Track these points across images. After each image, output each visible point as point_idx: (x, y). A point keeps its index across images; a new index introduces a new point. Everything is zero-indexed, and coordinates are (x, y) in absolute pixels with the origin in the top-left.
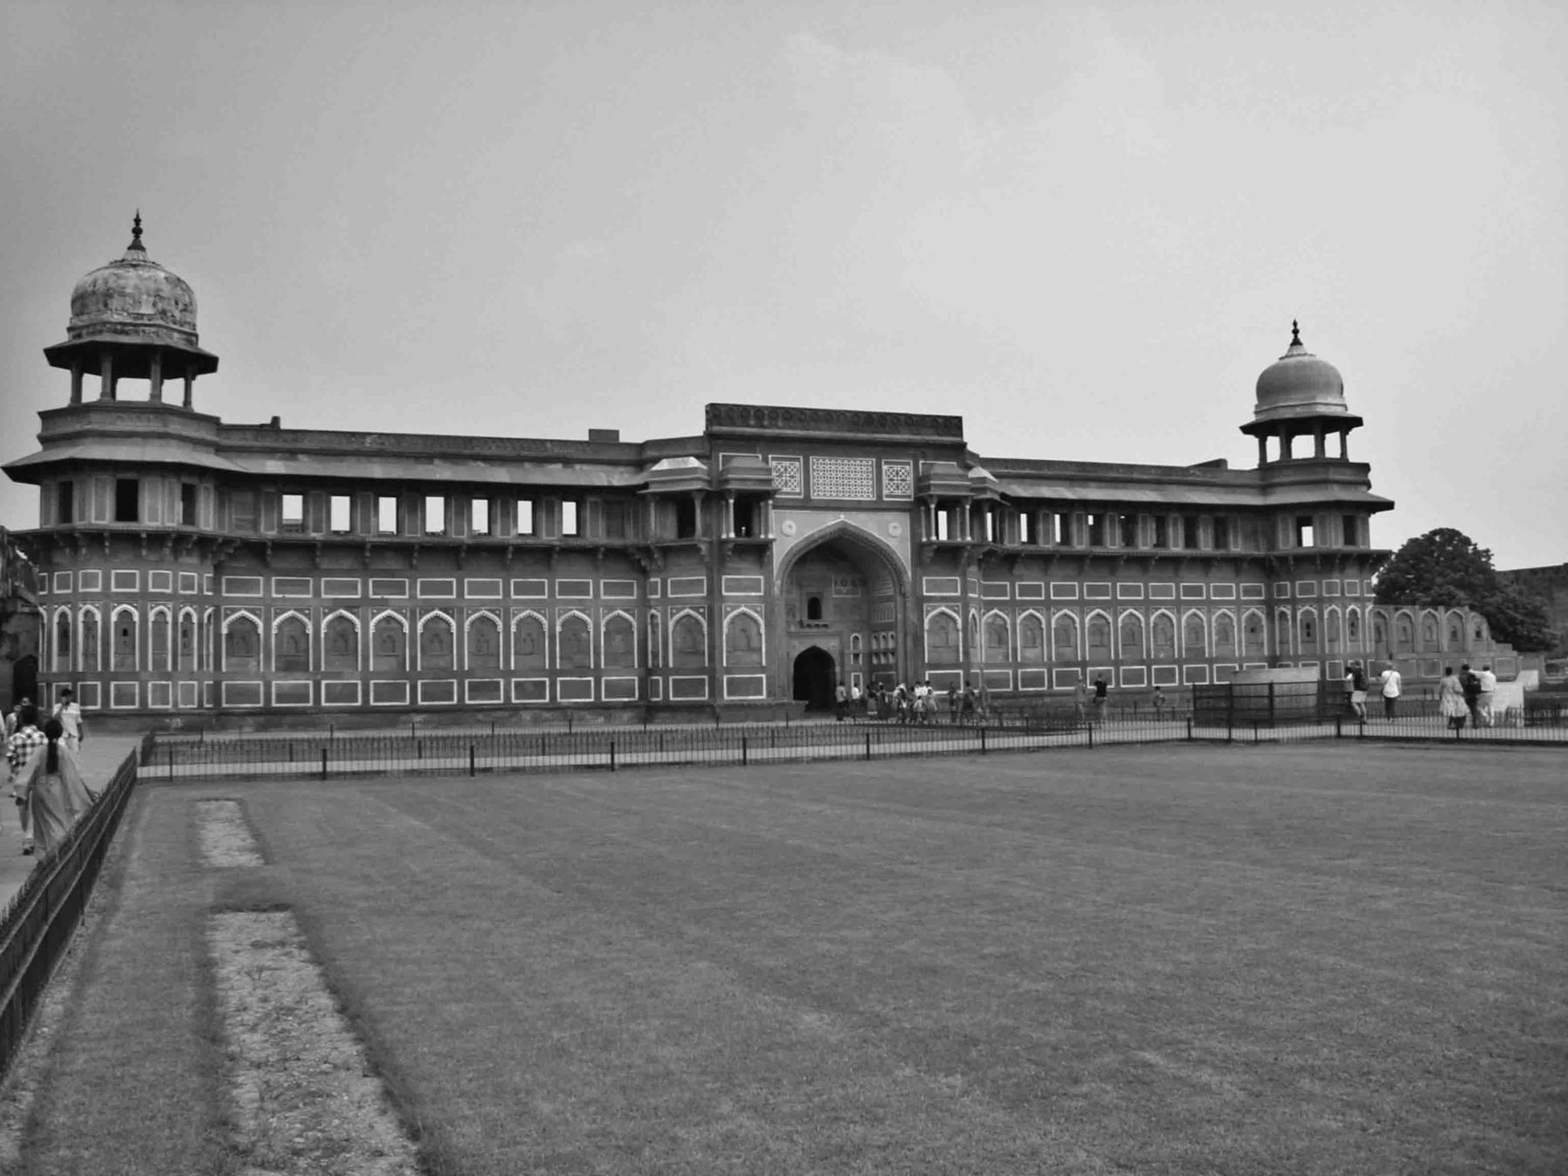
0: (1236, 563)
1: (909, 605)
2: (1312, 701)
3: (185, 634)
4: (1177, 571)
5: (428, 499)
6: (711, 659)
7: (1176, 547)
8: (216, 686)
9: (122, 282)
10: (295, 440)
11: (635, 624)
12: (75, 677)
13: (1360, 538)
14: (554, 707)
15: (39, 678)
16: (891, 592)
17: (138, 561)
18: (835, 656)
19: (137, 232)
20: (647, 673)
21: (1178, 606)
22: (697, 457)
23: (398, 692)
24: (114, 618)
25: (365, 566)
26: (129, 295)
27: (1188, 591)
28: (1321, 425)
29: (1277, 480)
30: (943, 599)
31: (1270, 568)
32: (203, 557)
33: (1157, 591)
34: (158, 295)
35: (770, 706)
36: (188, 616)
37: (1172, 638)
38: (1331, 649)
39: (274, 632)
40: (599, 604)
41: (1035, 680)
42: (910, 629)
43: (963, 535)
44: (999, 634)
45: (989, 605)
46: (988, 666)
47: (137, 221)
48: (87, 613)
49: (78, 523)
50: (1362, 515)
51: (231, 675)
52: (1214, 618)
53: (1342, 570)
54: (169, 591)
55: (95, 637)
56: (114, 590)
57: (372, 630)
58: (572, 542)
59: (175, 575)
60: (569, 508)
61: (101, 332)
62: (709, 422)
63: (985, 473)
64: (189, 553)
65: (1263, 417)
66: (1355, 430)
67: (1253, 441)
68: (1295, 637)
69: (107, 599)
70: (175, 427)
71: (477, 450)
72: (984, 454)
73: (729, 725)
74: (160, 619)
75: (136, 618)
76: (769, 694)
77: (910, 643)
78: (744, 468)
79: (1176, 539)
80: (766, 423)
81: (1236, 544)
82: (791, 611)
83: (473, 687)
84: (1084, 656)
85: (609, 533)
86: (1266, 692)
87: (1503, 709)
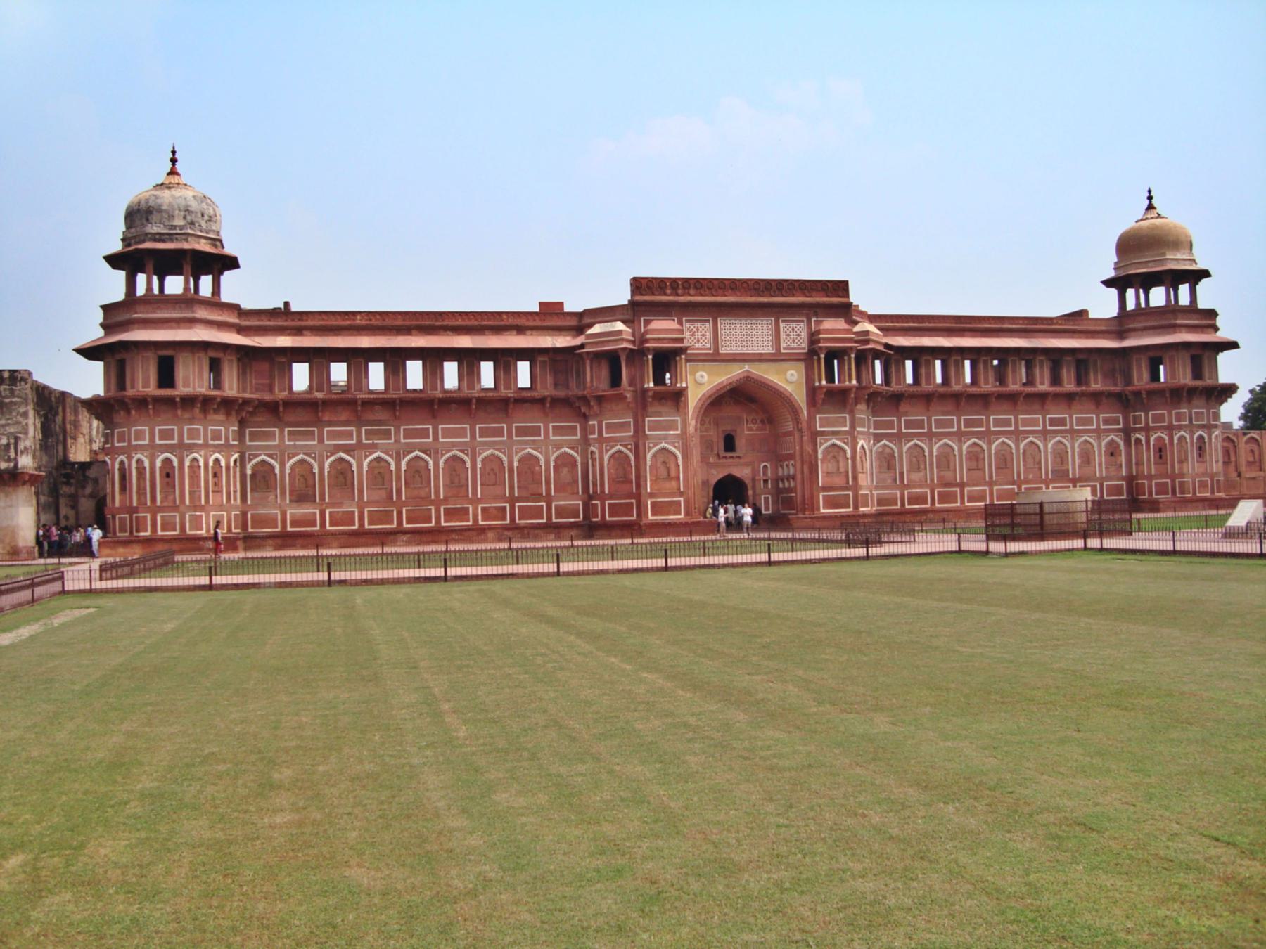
0: (1096, 397)
1: (805, 438)
2: (1082, 518)
3: (215, 475)
4: (1043, 404)
5: (409, 363)
6: (638, 486)
7: (1043, 387)
8: (244, 514)
9: (159, 201)
10: (300, 320)
11: (579, 459)
12: (132, 510)
13: (1206, 374)
14: (513, 527)
15: (107, 511)
16: (790, 428)
17: (176, 420)
18: (747, 482)
19: (174, 161)
20: (588, 498)
21: (1045, 434)
22: (624, 322)
23: (385, 516)
24: (158, 464)
25: (358, 418)
26: (166, 211)
27: (1052, 422)
28: (1173, 279)
29: (1132, 326)
31: (1126, 401)
32: (228, 414)
33: (1025, 423)
34: (188, 210)
35: (687, 523)
36: (217, 461)
37: (1040, 463)
38: (1181, 469)
39: (288, 471)
40: (548, 444)
41: (920, 499)
42: (806, 458)
43: (850, 380)
44: (888, 462)
45: (878, 438)
46: (877, 488)
47: (174, 152)
48: (139, 461)
49: (130, 392)
51: (253, 506)
52: (1076, 445)
53: (1189, 401)
54: (201, 442)
55: (145, 479)
56: (158, 442)
57: (365, 468)
58: (525, 394)
59: (206, 430)
60: (523, 368)
61: (144, 241)
62: (633, 293)
63: (871, 328)
64: (216, 411)
65: (1122, 273)
66: (1204, 282)
67: (1113, 293)
68: (1149, 460)
69: (153, 449)
70: (202, 313)
71: (445, 323)
72: (870, 312)
73: (640, 541)
75: (175, 463)
76: (687, 513)
77: (806, 470)
78: (662, 328)
79: (1042, 376)
80: (680, 292)
81: (1096, 382)
82: (707, 445)
83: (447, 512)
84: (962, 477)
85: (556, 385)
86: (1038, 511)
87: (1243, 523)
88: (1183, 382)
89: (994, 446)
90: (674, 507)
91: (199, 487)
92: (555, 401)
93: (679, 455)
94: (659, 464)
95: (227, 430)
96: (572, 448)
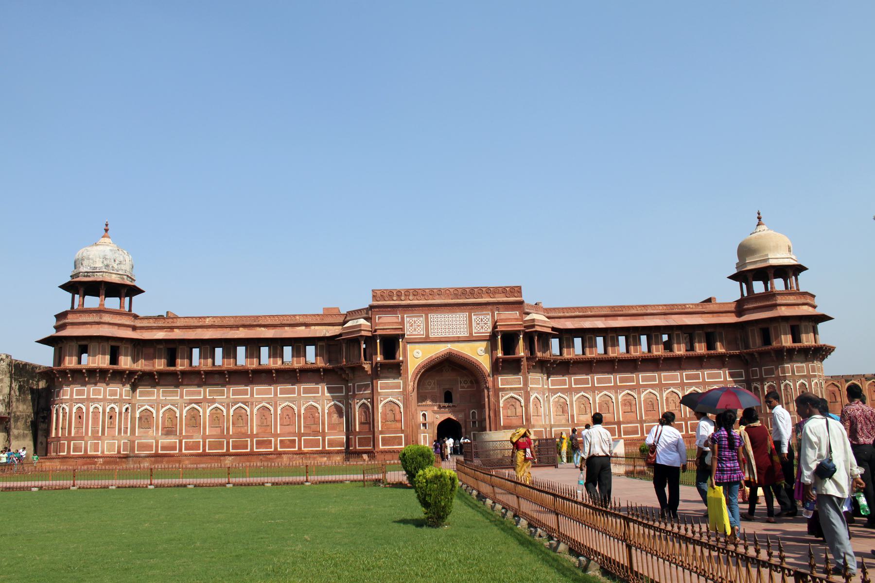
1: (491, 393)
5: (239, 348)
12: (58, 438)
14: (300, 453)
17: (84, 384)
18: (461, 423)
19: (106, 230)
22: (366, 319)
24: (74, 410)
30: (511, 389)
39: (161, 415)
44: (563, 408)
45: (554, 392)
47: (107, 225)
49: (62, 367)
50: (803, 325)
51: (140, 437)
56: (75, 397)
60: (311, 350)
70: (107, 318)
71: (259, 323)
72: (545, 307)
74: (96, 410)
75: (84, 410)
76: (406, 444)
77: (492, 415)
80: (403, 298)
83: (258, 443)
88: (784, 344)
89: (642, 396)
90: (398, 441)
91: (98, 424)
92: (326, 370)
93: (401, 405)
94: (388, 412)
95: (121, 390)
96: (339, 401)
